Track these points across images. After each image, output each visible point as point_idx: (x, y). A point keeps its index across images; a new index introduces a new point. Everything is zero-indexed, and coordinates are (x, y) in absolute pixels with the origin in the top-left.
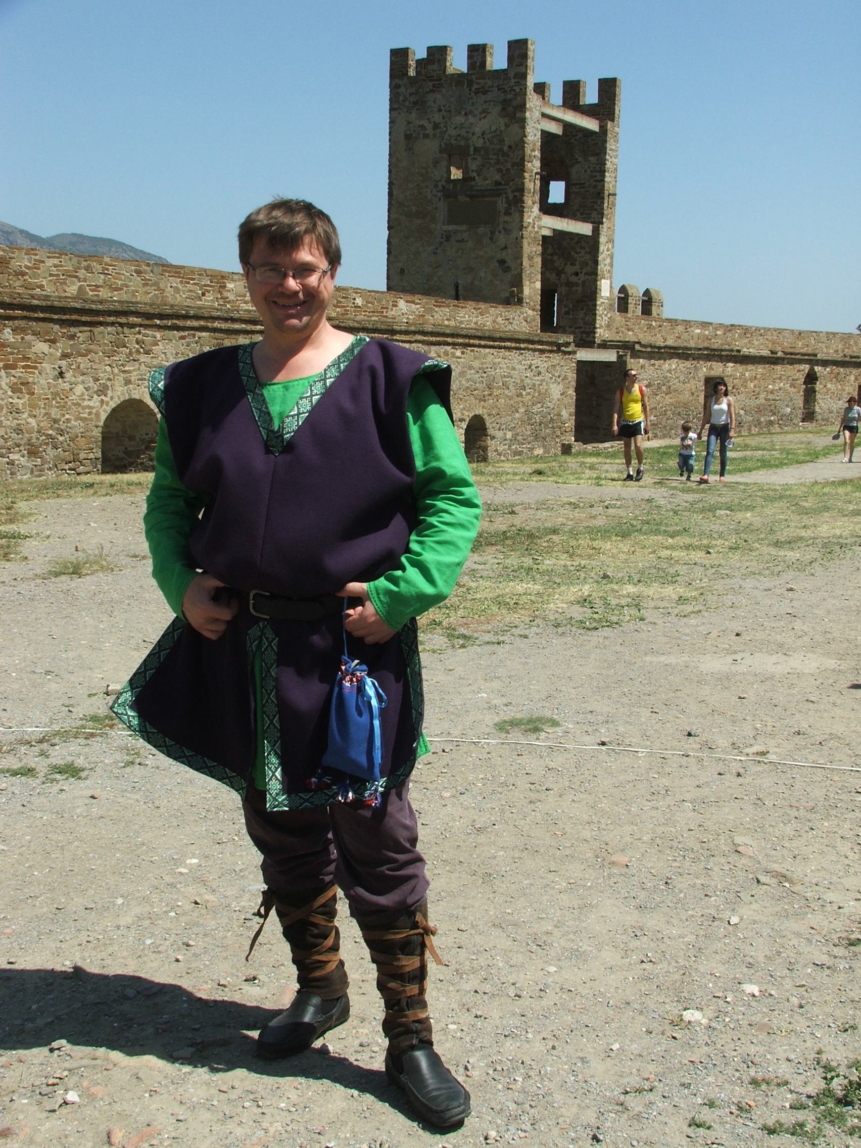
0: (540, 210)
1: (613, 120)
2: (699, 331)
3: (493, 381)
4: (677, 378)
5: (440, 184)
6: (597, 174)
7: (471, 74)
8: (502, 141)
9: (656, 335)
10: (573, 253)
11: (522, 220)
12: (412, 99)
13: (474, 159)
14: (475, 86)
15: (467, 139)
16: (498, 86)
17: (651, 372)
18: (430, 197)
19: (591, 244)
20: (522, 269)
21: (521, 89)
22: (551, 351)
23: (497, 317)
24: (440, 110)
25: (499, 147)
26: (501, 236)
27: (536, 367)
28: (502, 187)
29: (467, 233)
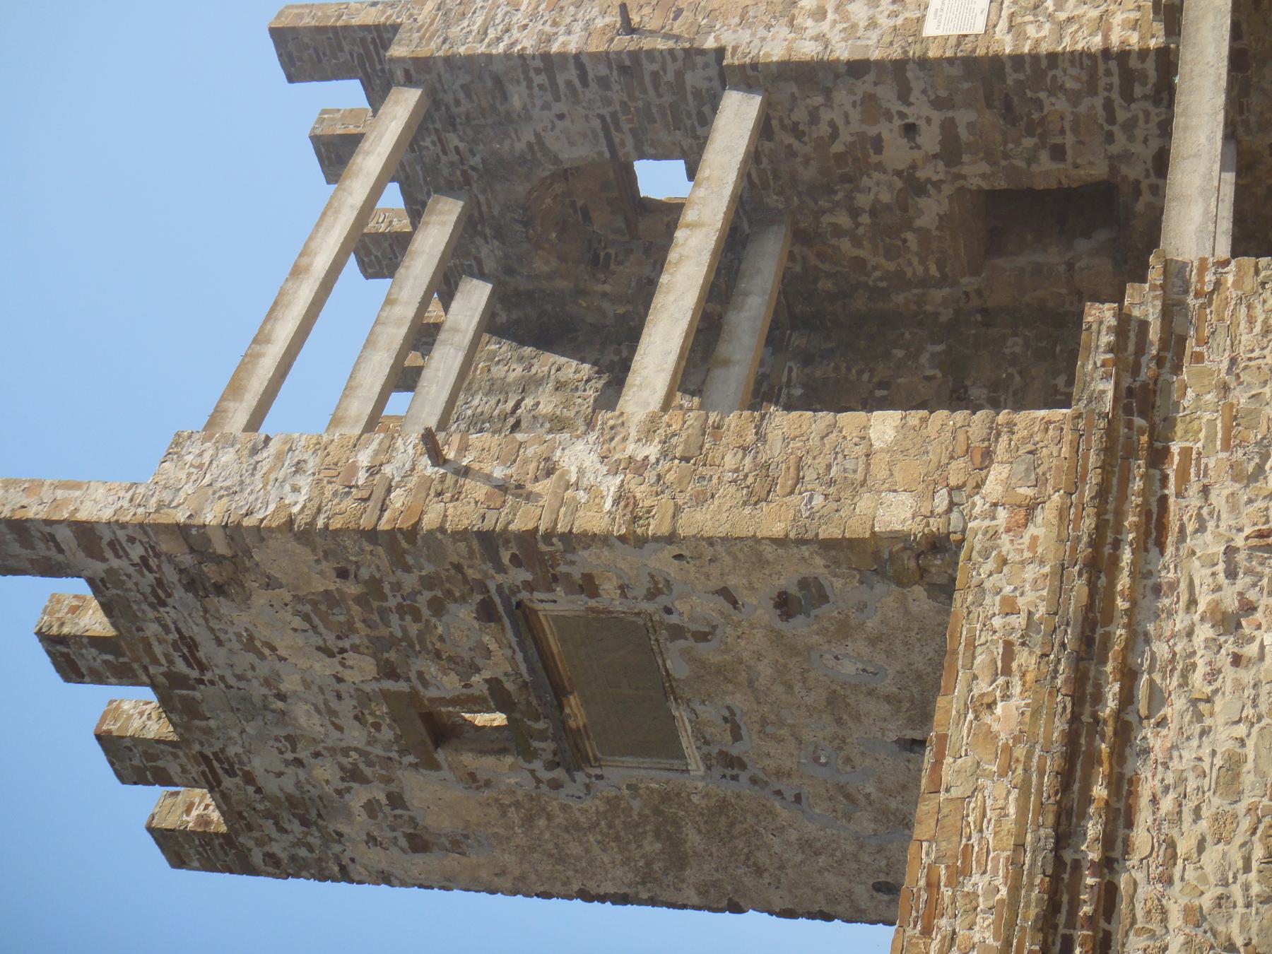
6: (561, 79)
10: (837, 148)
11: (604, 540)
12: (296, 827)
13: (425, 684)
14: (181, 666)
15: (364, 699)
18: (593, 805)
20: (801, 542)
21: (132, 540)
22: (1158, 456)
23: (991, 736)
24: (299, 763)
25: (356, 609)
26: (679, 606)
27: (1231, 574)
29: (699, 708)
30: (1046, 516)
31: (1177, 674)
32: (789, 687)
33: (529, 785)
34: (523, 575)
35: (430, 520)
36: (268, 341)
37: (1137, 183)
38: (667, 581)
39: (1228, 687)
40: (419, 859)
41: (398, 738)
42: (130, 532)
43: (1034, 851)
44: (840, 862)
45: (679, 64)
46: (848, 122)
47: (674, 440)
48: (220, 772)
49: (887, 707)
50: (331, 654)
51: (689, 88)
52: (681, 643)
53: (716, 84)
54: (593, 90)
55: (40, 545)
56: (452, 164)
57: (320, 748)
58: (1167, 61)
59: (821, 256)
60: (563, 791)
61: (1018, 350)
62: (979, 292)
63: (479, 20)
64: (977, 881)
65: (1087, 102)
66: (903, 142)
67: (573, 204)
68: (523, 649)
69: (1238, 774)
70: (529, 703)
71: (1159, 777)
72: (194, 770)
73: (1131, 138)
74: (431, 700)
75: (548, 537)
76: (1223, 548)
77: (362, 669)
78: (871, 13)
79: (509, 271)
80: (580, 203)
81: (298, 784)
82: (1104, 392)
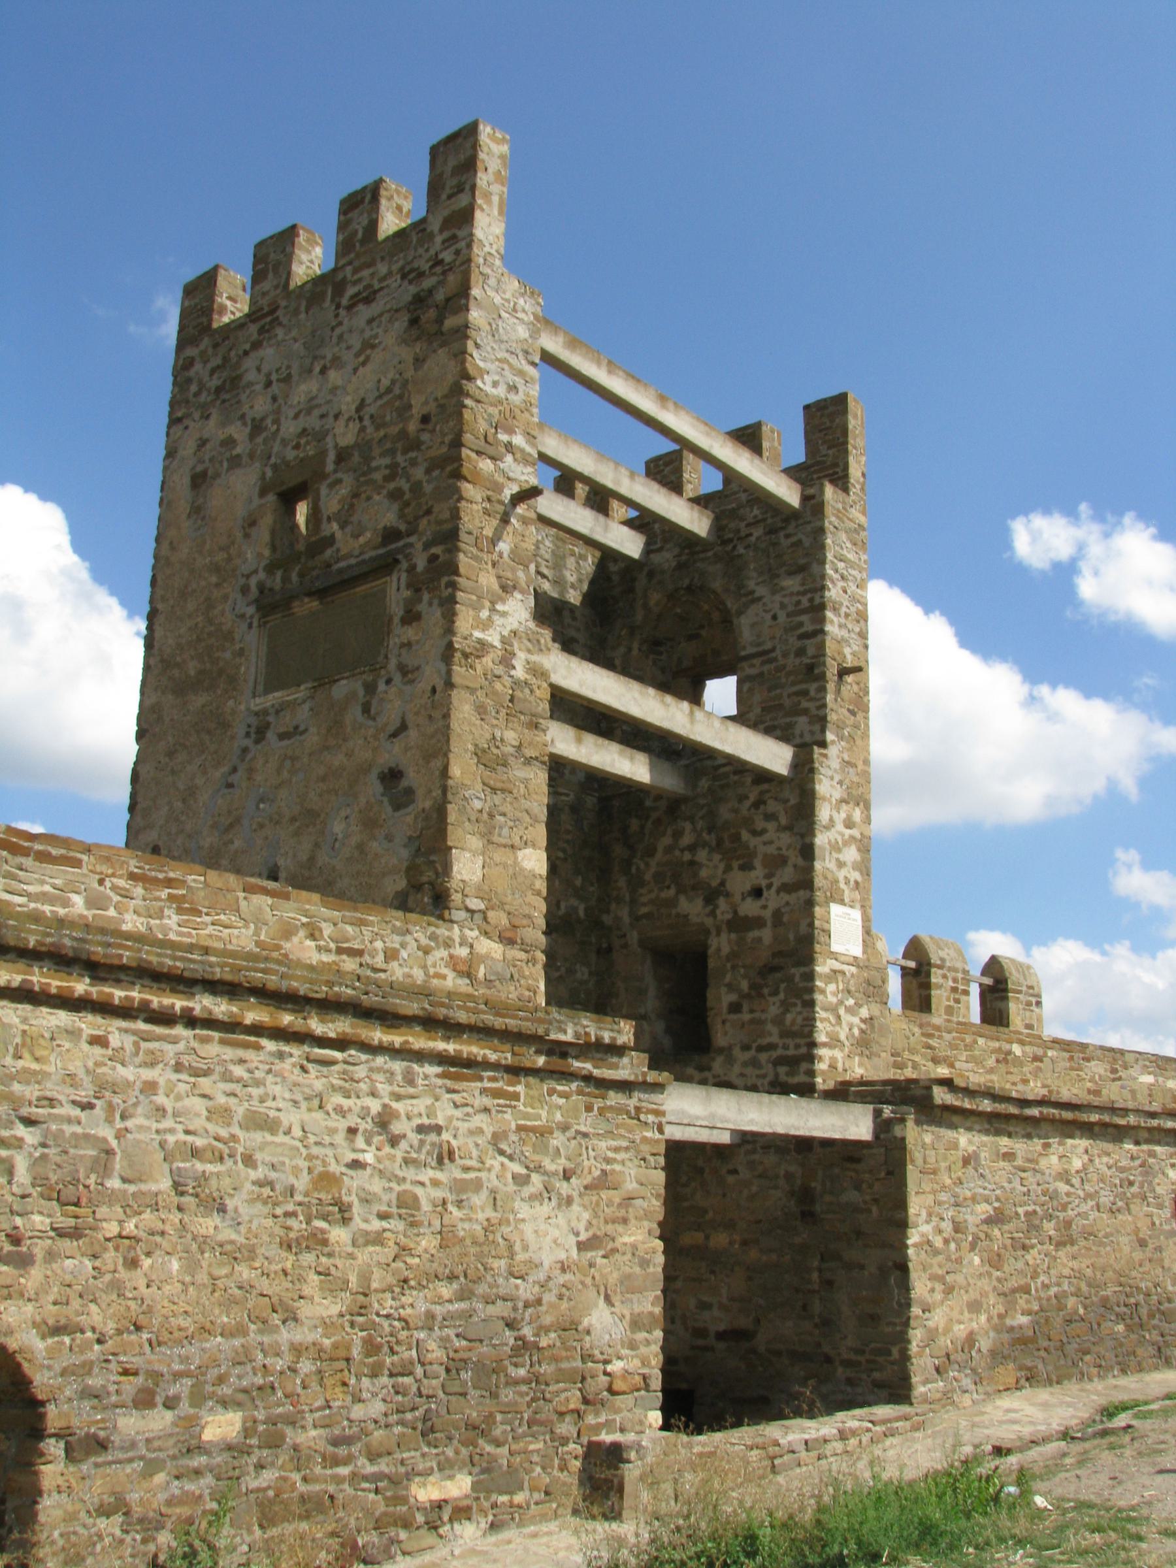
4: (1088, 1196)
6: (804, 618)
10: (745, 835)
11: (450, 630)
12: (215, 382)
13: (331, 486)
14: (351, 291)
15: (320, 436)
17: (1001, 1178)
20: (445, 789)
21: (457, 253)
22: (515, 1071)
24: (269, 384)
25: (394, 430)
26: (393, 690)
27: (421, 1129)
29: (307, 706)
30: (463, 985)
31: (341, 1083)
32: (323, 779)
33: (245, 569)
34: (421, 563)
35: (468, 489)
36: (610, 372)
37: (709, 1069)
38: (413, 681)
39: (331, 1124)
40: (187, 480)
41: (287, 464)
42: (464, 251)
43: (201, 962)
45: (814, 712)
46: (765, 844)
47: (527, 691)
48: (262, 322)
49: (305, 858)
50: (358, 410)
51: (794, 719)
52: (361, 692)
53: (798, 741)
54: (793, 642)
55: (454, 182)
56: (738, 531)
57: (281, 401)
58: (806, 1090)
59: (658, 821)
60: (239, 596)
61: (579, 975)
62: (625, 946)
63: (851, 556)
64: (172, 920)
65: (775, 1030)
66: (748, 887)
67: (702, 627)
68: (359, 564)
69: (262, 1129)
70: (314, 569)
71: (261, 1066)
72: (264, 302)
73: (745, 1064)
74: (318, 490)
75: (453, 585)
76: (441, 1123)
77: (345, 435)
78: (849, 864)
79: (651, 574)
80: (703, 633)
81: (250, 384)
82: (565, 1032)
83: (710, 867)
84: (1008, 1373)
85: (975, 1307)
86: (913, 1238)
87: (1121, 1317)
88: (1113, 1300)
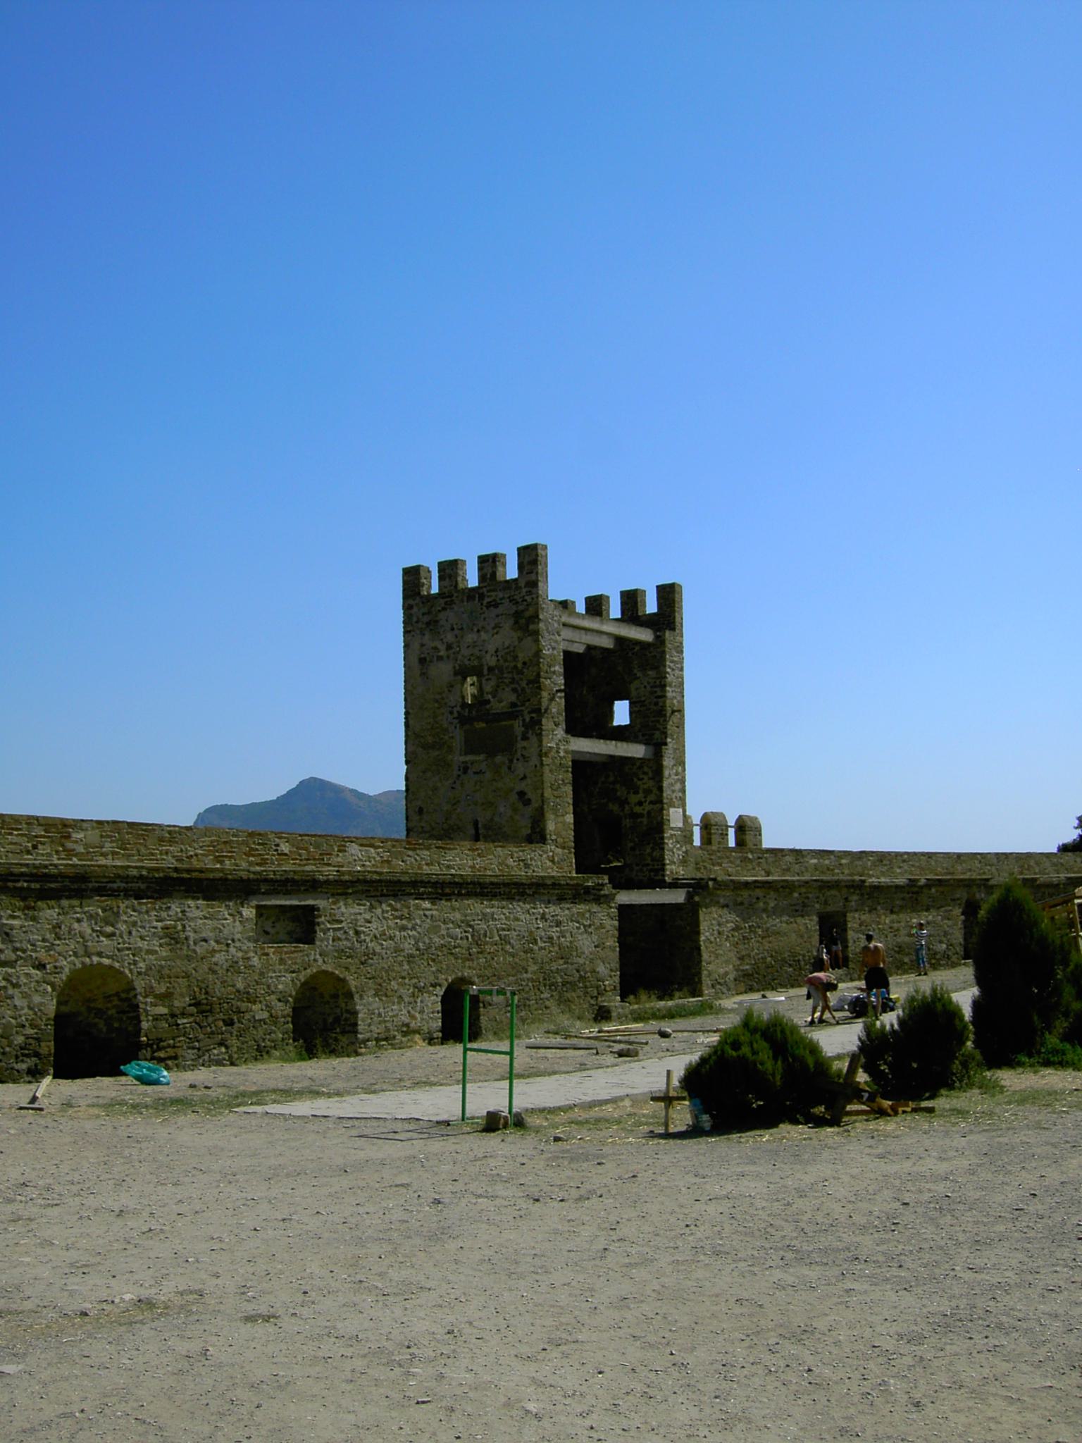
0: (568, 731)
1: (673, 629)
2: (814, 861)
3: (485, 935)
5: (455, 710)
6: (658, 689)
7: (482, 588)
8: (516, 658)
9: (754, 869)
10: (635, 780)
11: (540, 745)
12: (426, 619)
13: (487, 680)
15: (479, 658)
16: (509, 597)
19: (654, 767)
20: (543, 801)
21: (533, 599)
23: (506, 858)
25: (512, 664)
26: (520, 765)
27: (553, 916)
28: (518, 709)
29: (484, 763)
34: (528, 720)
44: (430, 798)
50: (496, 652)
52: (507, 762)
65: (649, 859)
66: (637, 801)
75: (541, 729)
77: (492, 661)
81: (443, 626)
83: (621, 792)
84: (742, 987)
85: (727, 962)
86: (702, 938)
87: (790, 966)
88: (788, 958)
